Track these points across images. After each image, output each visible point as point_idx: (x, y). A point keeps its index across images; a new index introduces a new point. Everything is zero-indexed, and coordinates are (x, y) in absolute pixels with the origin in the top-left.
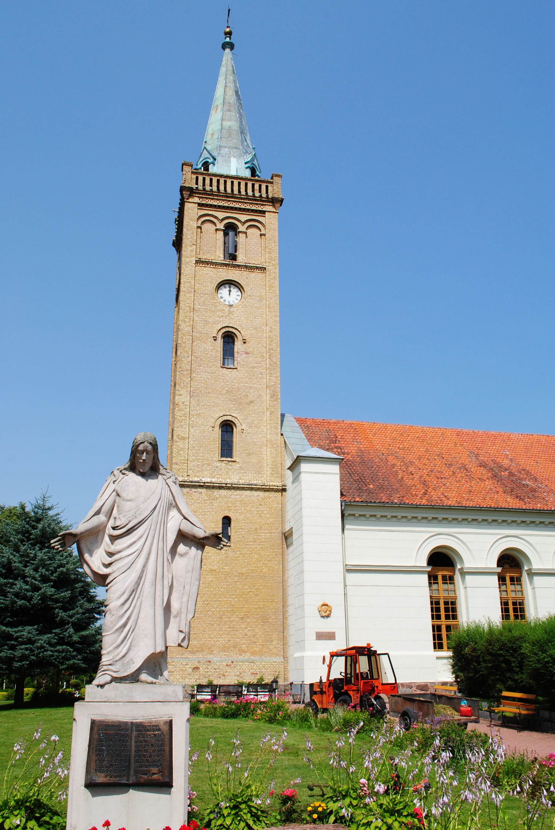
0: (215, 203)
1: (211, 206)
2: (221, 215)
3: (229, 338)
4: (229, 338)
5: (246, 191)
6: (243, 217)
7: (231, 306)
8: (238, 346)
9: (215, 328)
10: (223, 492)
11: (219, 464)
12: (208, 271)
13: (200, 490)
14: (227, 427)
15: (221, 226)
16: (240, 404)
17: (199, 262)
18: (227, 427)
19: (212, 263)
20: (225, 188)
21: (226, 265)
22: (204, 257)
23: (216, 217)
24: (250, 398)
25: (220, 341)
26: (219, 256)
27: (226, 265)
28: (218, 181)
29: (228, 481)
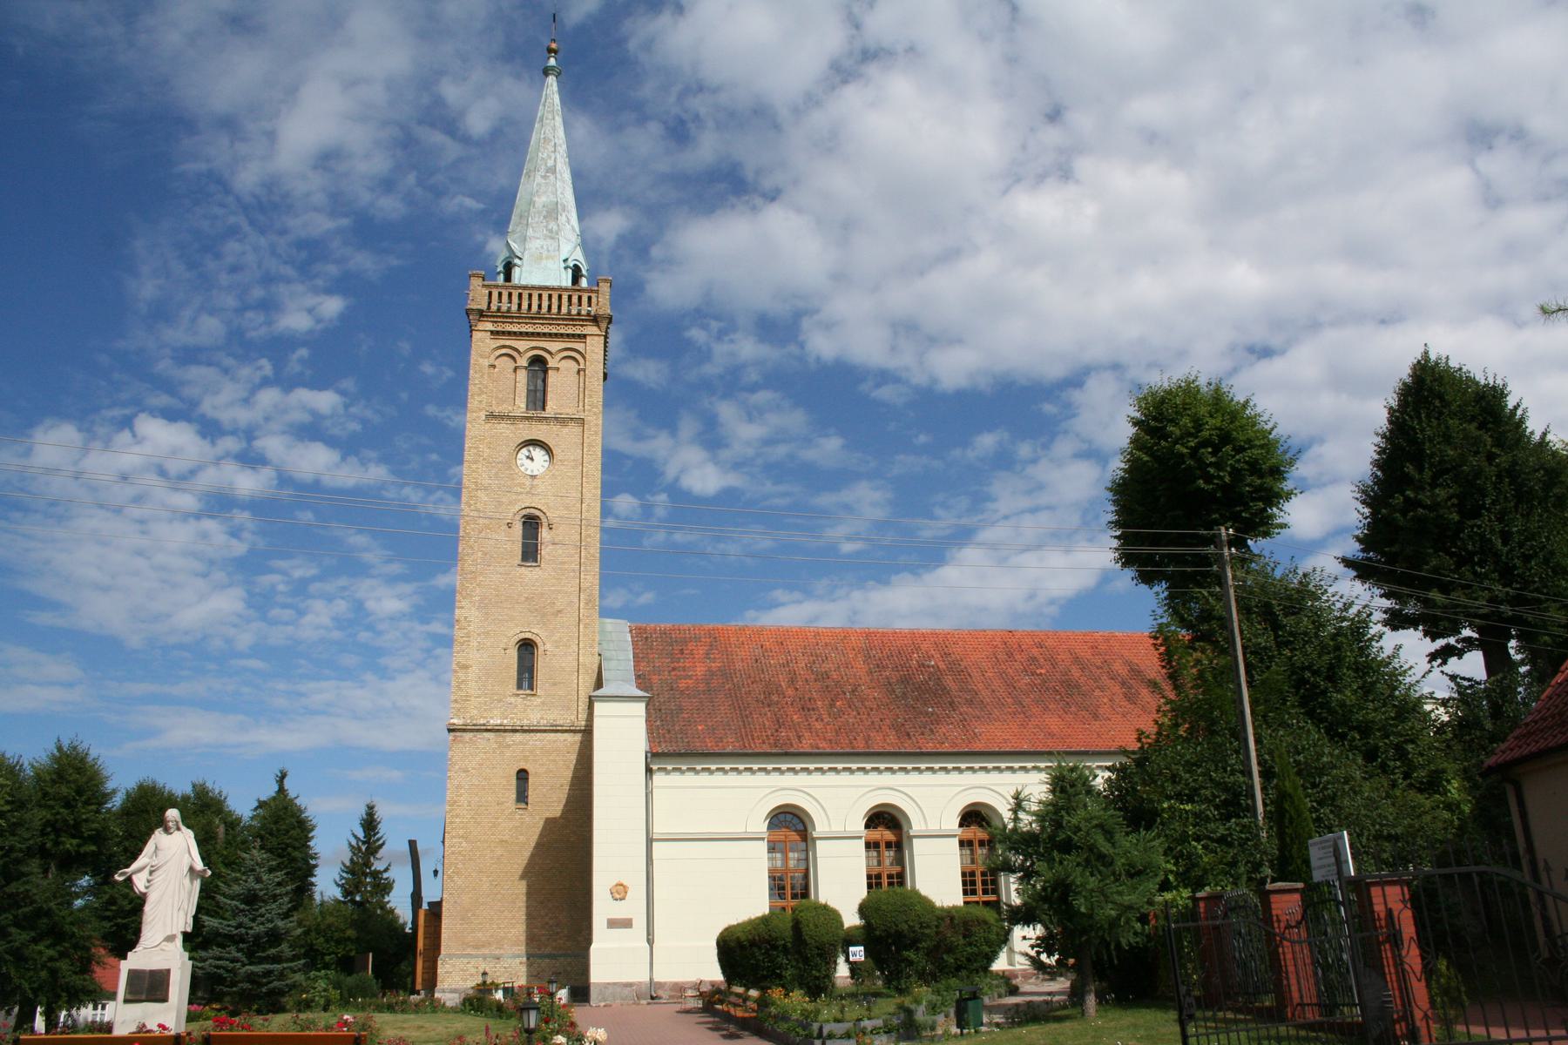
0: (515, 328)
1: (509, 333)
2: (522, 345)
3: (531, 524)
4: (531, 524)
5: (560, 307)
6: (554, 346)
7: (533, 477)
8: (544, 534)
9: (513, 512)
10: (518, 737)
11: (513, 700)
12: (503, 428)
13: (486, 735)
14: (527, 647)
15: (523, 362)
16: (544, 615)
17: (491, 416)
18: (527, 647)
19: (509, 417)
20: (530, 306)
21: (527, 418)
22: (497, 410)
23: (516, 350)
24: (559, 606)
25: (518, 528)
26: (521, 403)
27: (527, 418)
28: (520, 295)
29: (525, 722)
